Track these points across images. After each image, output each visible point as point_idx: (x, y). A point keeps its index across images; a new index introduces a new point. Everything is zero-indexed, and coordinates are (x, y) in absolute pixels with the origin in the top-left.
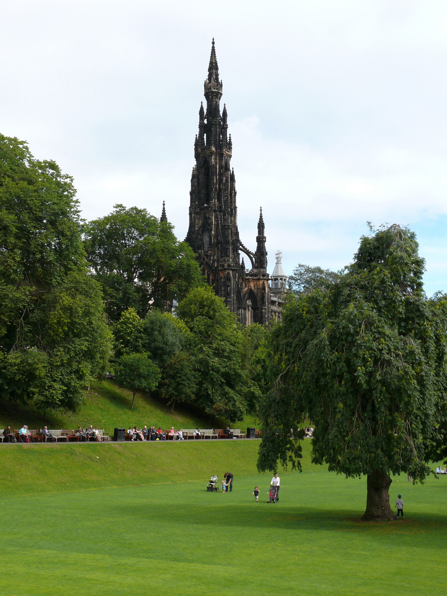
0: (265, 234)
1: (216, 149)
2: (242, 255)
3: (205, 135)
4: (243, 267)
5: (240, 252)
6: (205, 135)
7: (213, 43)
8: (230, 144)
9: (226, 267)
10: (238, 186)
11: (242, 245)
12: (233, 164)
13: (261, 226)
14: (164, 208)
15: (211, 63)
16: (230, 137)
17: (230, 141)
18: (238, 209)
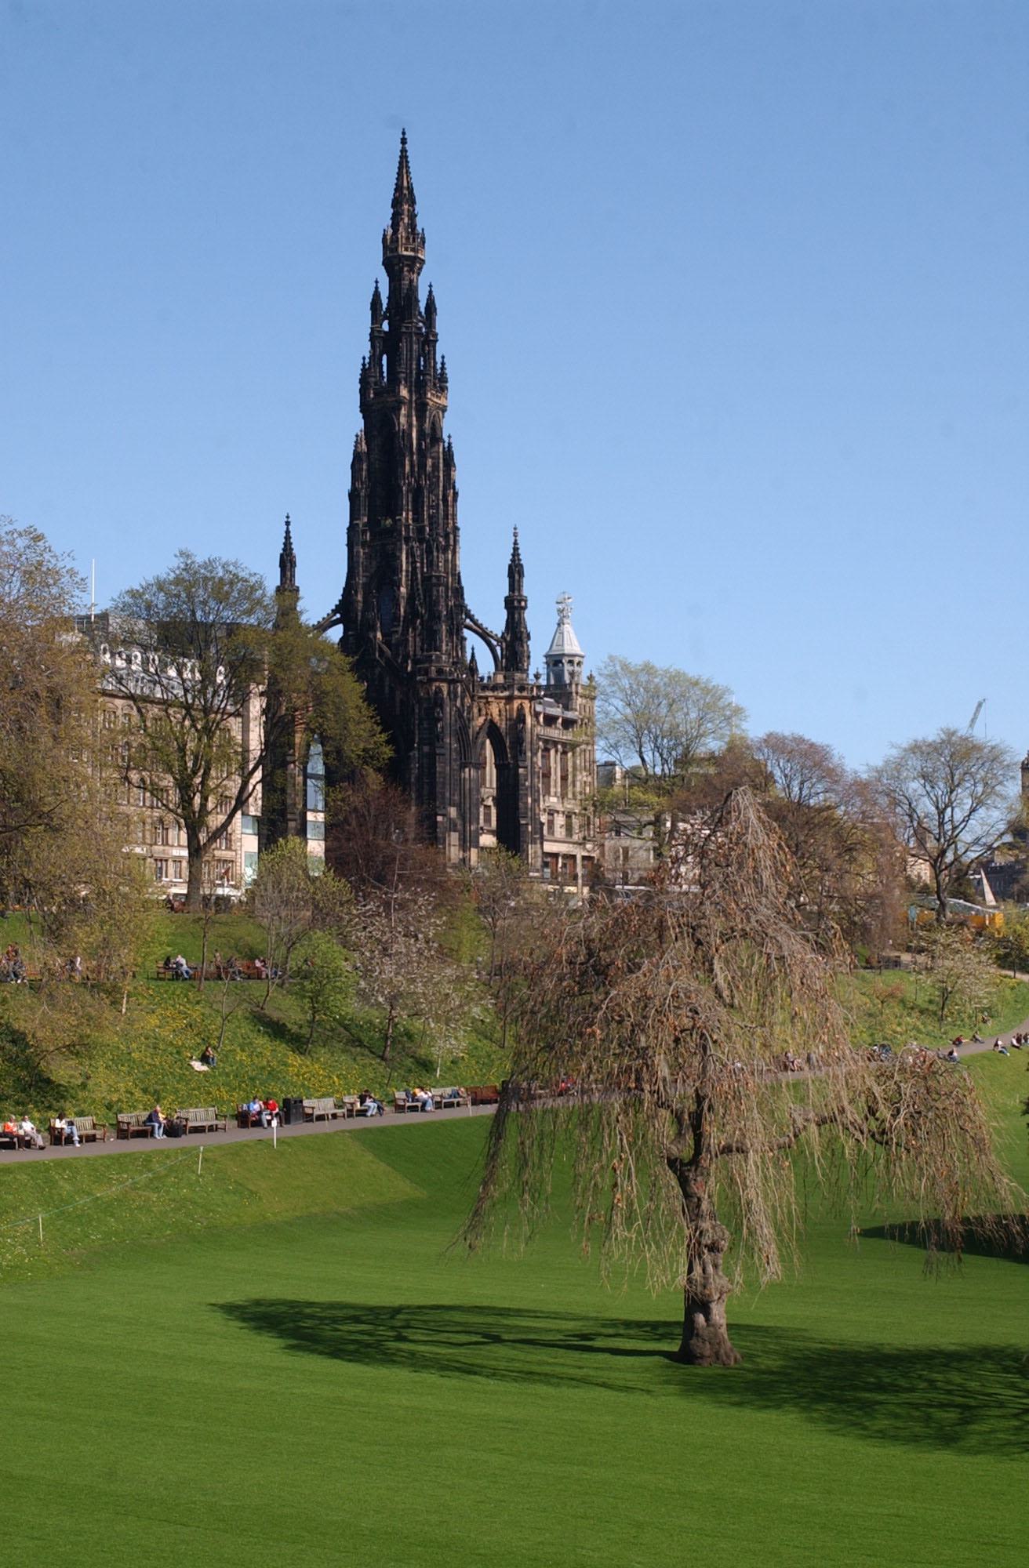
0: (526, 591)
1: (410, 392)
2: (472, 640)
3: (385, 357)
4: (472, 669)
5: (466, 633)
6: (385, 357)
7: (404, 141)
8: (443, 379)
9: (433, 675)
10: (462, 477)
11: (472, 618)
12: (449, 426)
13: (515, 571)
14: (288, 532)
15: (399, 188)
16: (443, 364)
17: (443, 374)
18: (461, 533)
